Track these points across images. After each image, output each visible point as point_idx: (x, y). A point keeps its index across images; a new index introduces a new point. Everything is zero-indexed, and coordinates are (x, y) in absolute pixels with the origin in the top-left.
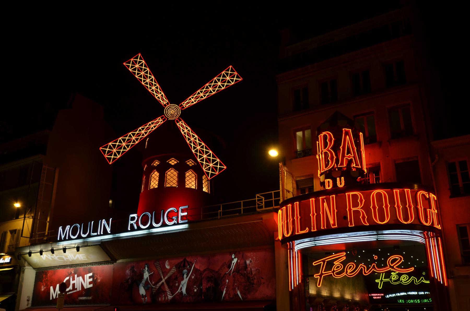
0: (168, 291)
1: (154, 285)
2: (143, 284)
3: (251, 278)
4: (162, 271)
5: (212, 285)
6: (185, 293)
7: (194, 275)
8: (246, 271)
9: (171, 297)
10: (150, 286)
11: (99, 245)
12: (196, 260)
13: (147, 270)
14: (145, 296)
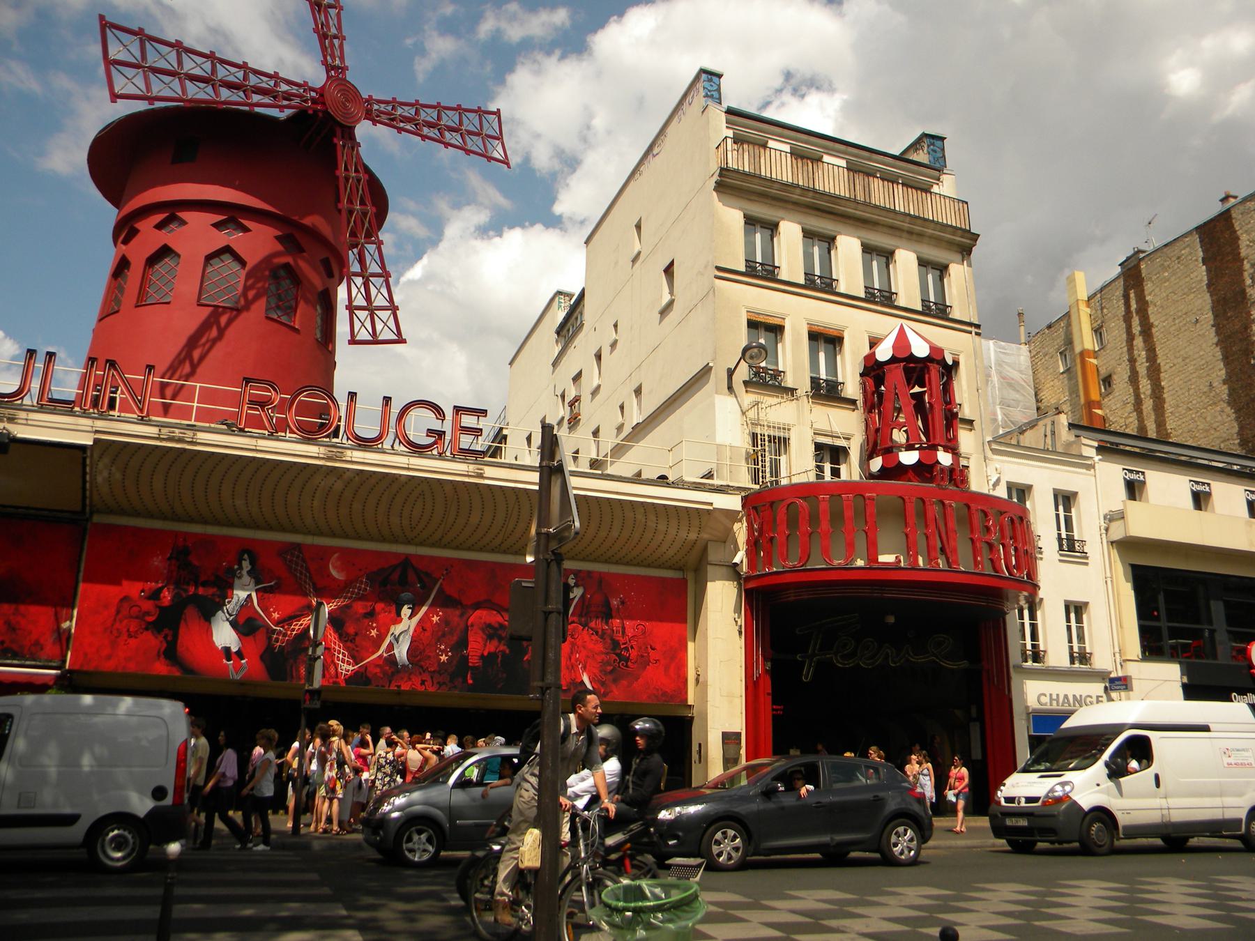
0: (337, 648)
1: (277, 623)
2: (231, 615)
3: (625, 644)
4: (314, 585)
5: (502, 647)
6: (407, 663)
7: (440, 613)
8: (607, 624)
9: (351, 668)
10: (260, 623)
11: (82, 448)
12: (446, 570)
13: (249, 573)
14: (240, 654)
